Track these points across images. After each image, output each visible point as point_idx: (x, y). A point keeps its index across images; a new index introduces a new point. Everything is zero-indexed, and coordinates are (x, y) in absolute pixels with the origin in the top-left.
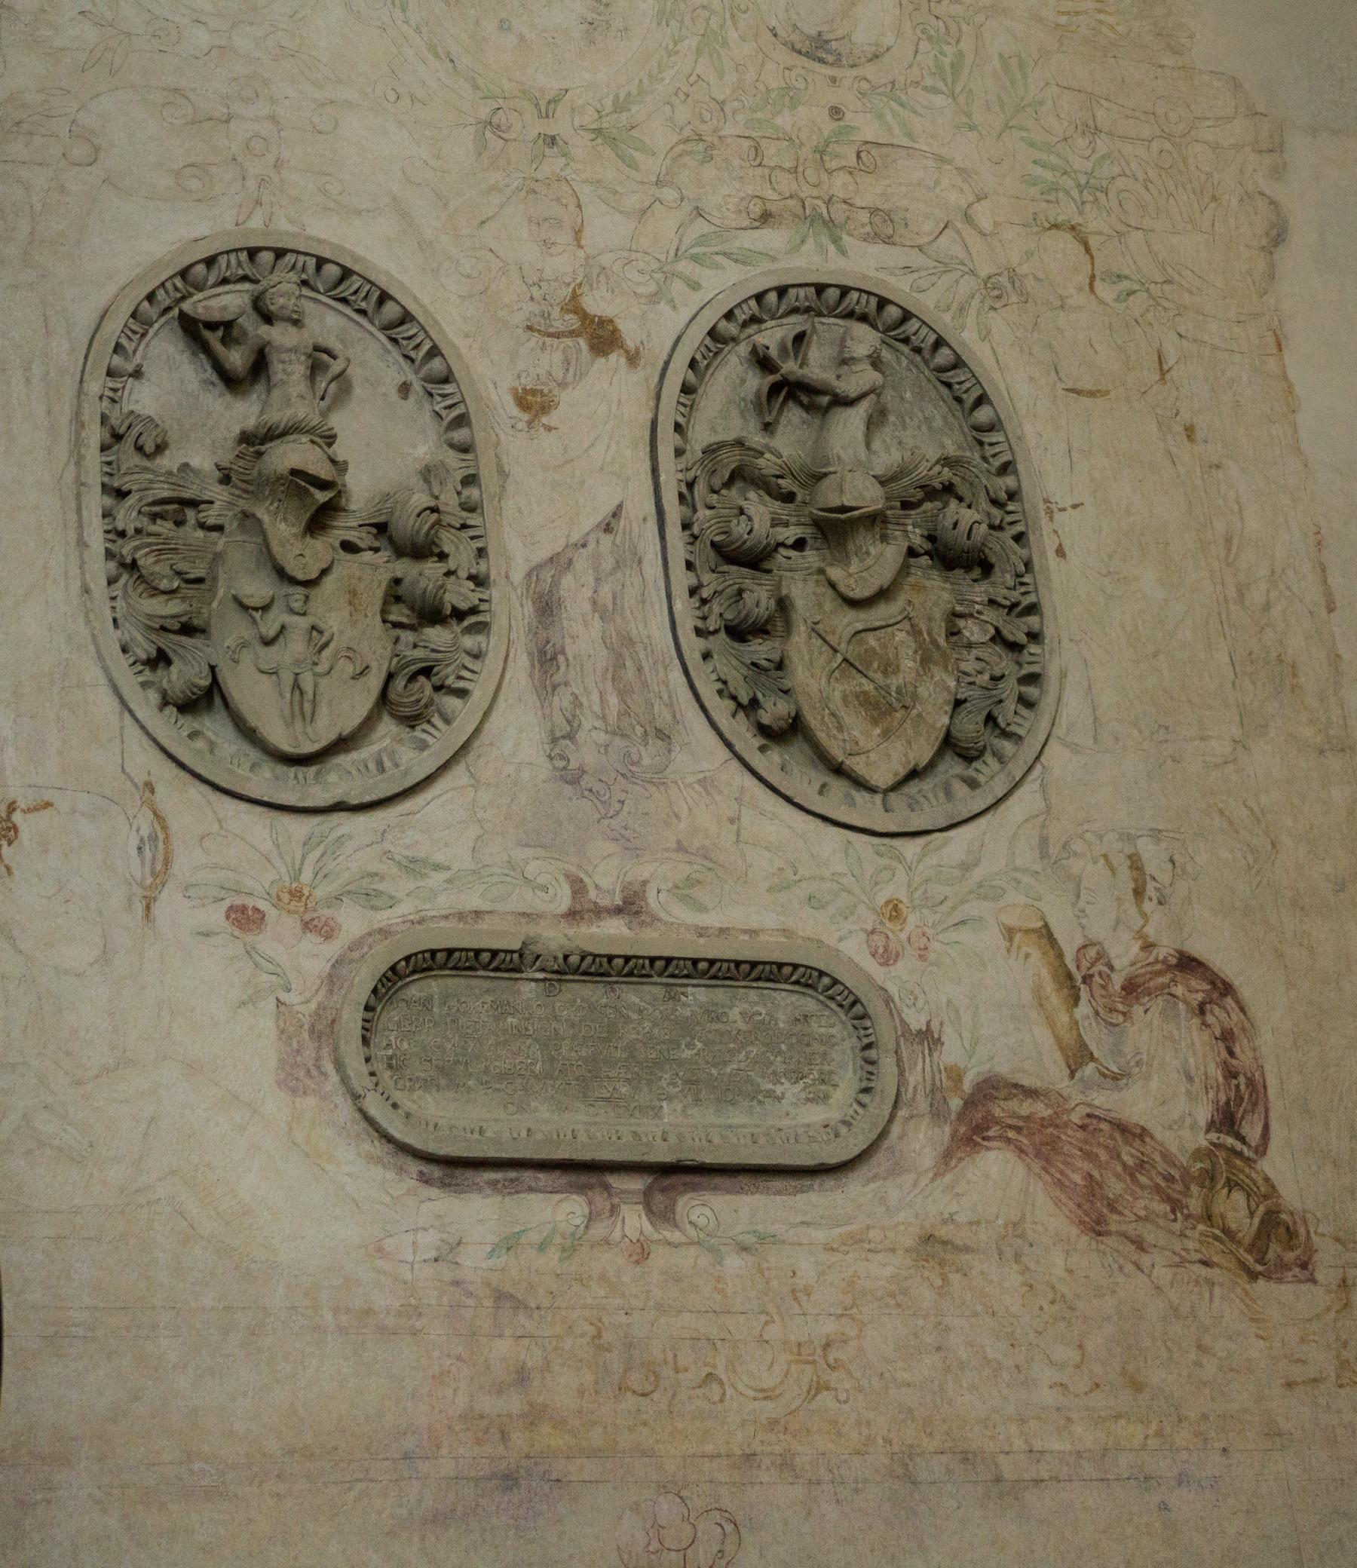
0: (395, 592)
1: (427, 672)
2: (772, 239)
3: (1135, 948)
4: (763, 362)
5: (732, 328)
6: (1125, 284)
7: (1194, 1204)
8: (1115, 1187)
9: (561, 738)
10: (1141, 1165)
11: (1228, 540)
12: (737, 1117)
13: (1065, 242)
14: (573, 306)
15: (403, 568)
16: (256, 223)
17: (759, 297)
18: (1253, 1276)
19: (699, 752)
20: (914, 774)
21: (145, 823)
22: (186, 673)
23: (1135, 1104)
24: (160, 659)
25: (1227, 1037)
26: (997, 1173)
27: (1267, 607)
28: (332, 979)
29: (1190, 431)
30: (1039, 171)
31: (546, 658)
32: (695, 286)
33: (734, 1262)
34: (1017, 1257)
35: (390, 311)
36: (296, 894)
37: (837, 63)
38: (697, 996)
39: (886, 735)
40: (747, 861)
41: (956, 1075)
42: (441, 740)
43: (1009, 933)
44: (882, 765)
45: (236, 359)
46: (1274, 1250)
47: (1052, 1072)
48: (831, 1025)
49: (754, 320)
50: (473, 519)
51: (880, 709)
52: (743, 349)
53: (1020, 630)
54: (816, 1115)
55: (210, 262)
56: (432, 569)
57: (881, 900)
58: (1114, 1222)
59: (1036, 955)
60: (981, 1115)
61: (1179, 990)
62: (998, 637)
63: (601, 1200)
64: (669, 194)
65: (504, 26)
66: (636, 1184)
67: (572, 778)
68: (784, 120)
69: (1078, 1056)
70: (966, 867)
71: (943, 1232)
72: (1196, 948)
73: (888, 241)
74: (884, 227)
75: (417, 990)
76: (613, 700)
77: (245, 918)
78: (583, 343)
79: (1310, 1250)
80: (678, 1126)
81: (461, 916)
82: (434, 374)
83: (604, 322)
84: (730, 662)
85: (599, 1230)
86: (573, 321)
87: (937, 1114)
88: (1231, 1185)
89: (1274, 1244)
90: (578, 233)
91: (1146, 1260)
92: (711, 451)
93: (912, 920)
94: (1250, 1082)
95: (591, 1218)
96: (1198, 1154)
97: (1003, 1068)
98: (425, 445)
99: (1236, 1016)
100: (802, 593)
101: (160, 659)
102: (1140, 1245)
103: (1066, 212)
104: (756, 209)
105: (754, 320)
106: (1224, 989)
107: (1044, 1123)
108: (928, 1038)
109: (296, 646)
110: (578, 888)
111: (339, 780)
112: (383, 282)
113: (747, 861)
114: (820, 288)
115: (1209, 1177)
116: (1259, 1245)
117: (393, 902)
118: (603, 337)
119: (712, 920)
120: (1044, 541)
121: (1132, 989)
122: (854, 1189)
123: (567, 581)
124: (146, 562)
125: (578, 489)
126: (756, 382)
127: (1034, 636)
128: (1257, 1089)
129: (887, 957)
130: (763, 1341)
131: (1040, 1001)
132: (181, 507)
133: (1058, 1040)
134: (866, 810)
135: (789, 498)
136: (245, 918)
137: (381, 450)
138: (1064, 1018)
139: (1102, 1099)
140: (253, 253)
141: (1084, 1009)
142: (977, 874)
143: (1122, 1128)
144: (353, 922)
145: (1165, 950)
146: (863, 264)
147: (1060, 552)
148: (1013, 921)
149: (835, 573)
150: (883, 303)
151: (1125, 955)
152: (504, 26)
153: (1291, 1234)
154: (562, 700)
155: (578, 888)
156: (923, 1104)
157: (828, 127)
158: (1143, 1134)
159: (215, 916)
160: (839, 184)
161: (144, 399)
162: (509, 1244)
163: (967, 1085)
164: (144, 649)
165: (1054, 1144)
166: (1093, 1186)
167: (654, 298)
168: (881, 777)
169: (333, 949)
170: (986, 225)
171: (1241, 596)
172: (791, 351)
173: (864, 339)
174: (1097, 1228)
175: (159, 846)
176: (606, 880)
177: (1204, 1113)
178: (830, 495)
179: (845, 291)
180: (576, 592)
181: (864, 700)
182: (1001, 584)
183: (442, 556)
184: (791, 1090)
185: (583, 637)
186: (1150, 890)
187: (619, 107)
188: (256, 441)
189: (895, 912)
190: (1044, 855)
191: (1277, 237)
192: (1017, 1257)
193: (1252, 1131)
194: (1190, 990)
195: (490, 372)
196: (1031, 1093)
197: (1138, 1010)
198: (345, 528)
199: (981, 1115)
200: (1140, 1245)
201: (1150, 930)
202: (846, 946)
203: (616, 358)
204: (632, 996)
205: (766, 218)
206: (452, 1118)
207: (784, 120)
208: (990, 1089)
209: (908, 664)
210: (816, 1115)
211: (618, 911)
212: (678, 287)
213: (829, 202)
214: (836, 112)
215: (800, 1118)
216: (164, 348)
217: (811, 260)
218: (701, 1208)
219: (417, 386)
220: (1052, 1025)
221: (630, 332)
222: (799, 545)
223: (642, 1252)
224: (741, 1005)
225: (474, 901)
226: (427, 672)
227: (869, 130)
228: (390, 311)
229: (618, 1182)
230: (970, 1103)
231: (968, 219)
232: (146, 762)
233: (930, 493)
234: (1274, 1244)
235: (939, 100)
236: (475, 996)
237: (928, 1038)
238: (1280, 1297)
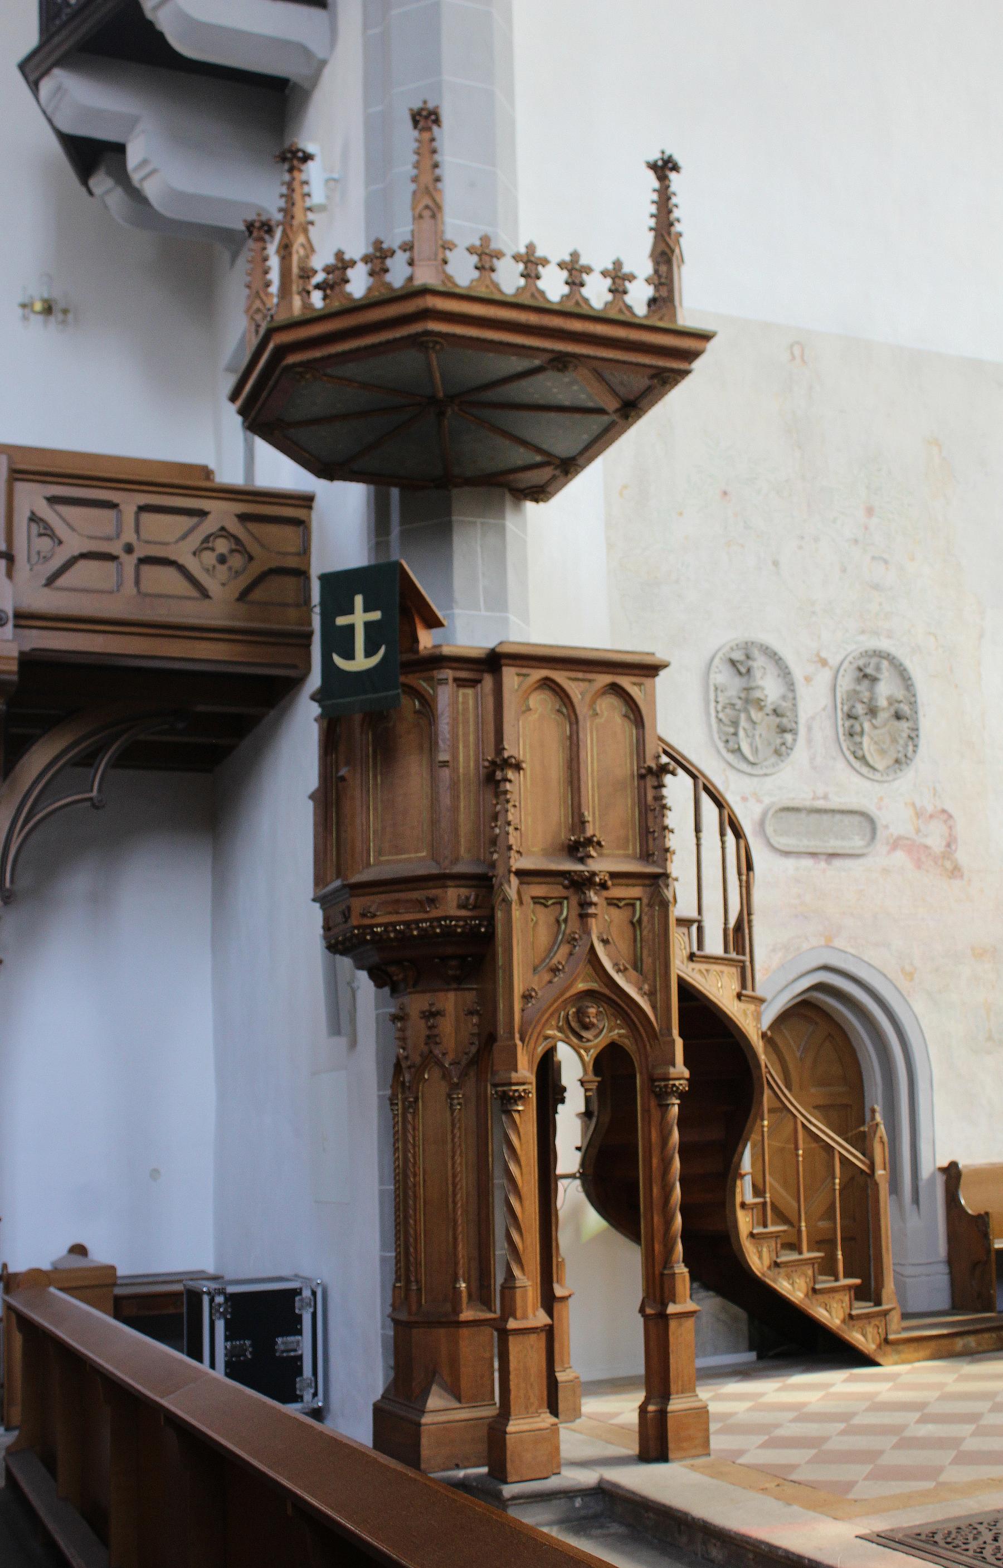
2: (862, 638)
9: (812, 759)
14: (818, 655)
19: (841, 764)
22: (732, 745)
23: (929, 841)
25: (950, 828)
26: (900, 857)
31: (809, 741)
38: (838, 817)
40: (850, 788)
43: (906, 804)
44: (880, 765)
45: (743, 670)
60: (896, 844)
69: (918, 831)
72: (946, 808)
80: (834, 844)
82: (785, 673)
89: (955, 872)
100: (867, 726)
108: (886, 827)
110: (814, 792)
113: (850, 788)
116: (952, 872)
118: (824, 663)
120: (921, 713)
121: (931, 816)
127: (917, 736)
143: (926, 847)
146: (884, 644)
151: (930, 809)
155: (814, 792)
166: (919, 859)
176: (820, 792)
177: (944, 843)
184: (857, 838)
189: (881, 799)
193: (953, 847)
194: (944, 817)
195: (798, 673)
196: (907, 839)
199: (896, 844)
200: (927, 871)
202: (871, 809)
203: (827, 669)
204: (825, 817)
208: (900, 838)
215: (857, 843)
237: (886, 827)
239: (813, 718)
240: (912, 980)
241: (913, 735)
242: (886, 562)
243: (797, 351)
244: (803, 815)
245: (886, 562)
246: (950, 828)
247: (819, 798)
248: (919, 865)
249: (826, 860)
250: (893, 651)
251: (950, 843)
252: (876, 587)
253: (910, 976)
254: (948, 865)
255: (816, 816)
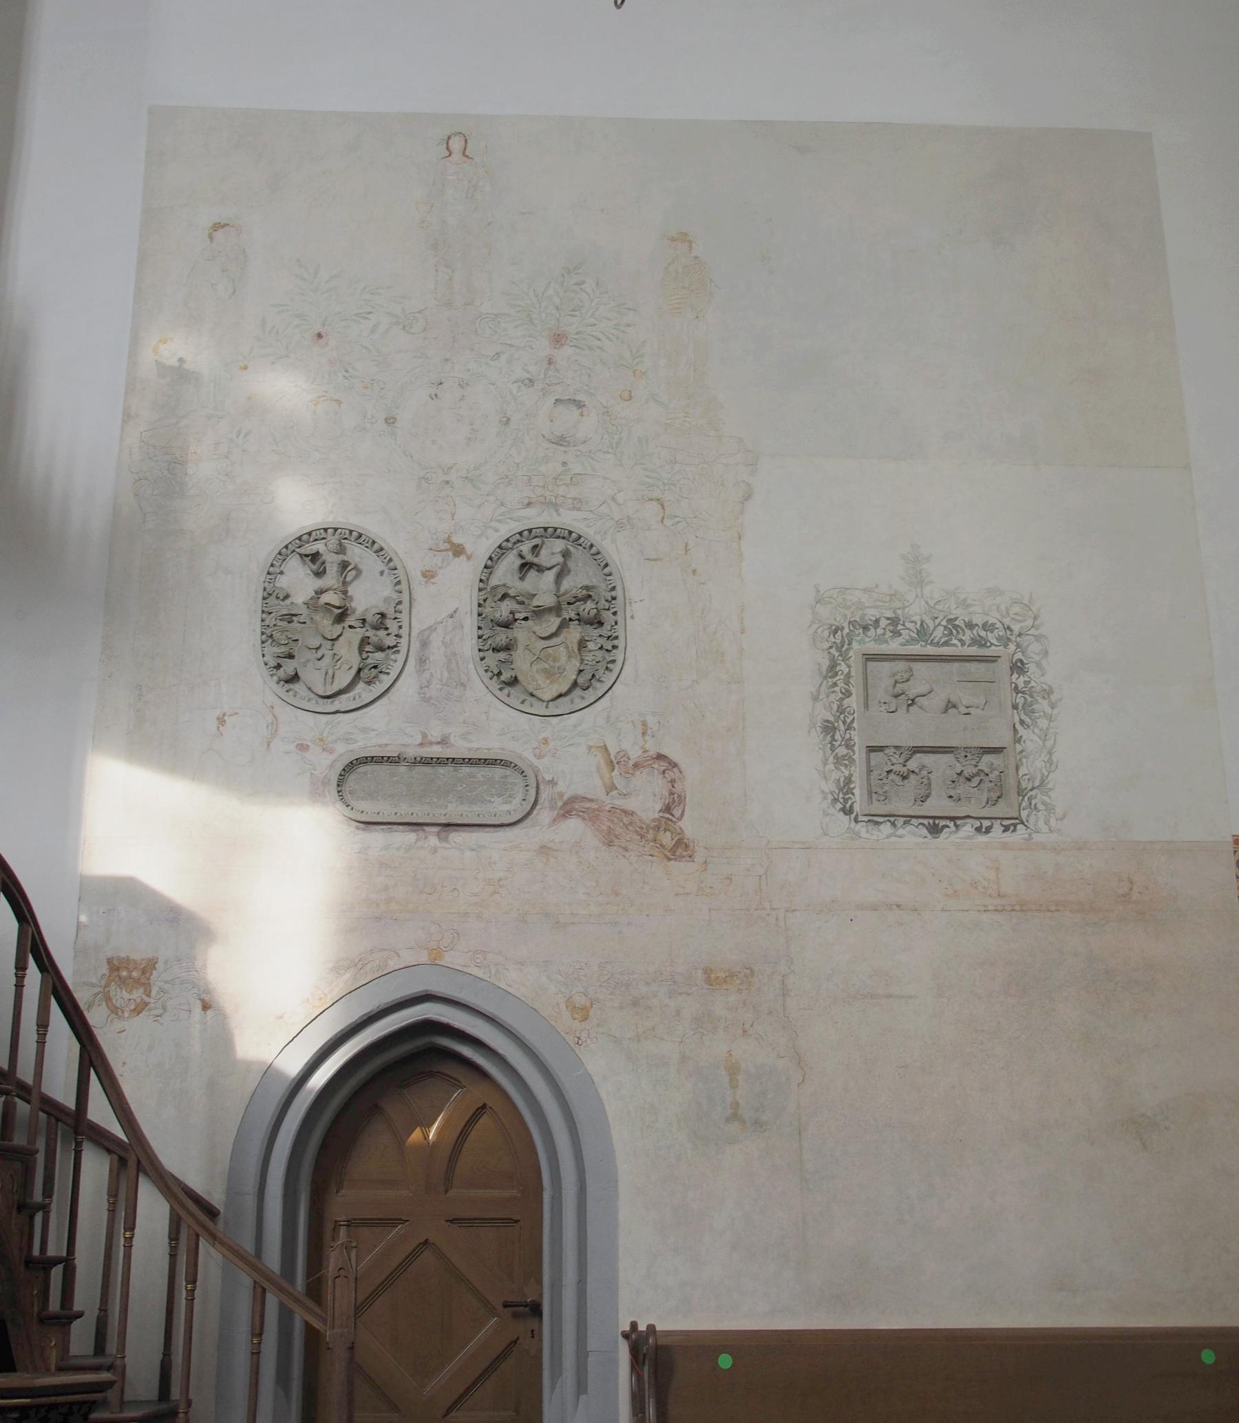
0: (364, 641)
1: (375, 667)
2: (531, 512)
3: (640, 752)
4: (521, 556)
5: (510, 545)
6: (677, 519)
7: (650, 836)
8: (619, 830)
10: (631, 823)
11: (703, 610)
12: (476, 808)
13: (655, 506)
14: (448, 541)
15: (370, 633)
16: (330, 519)
17: (521, 533)
18: (670, 860)
20: (560, 696)
21: (270, 718)
23: (630, 804)
24: (279, 666)
25: (673, 781)
26: (574, 826)
27: (715, 632)
28: (331, 766)
29: (694, 572)
30: (647, 480)
31: (422, 661)
32: (497, 531)
33: (468, 854)
34: (577, 853)
35: (376, 547)
36: (321, 740)
37: (568, 445)
38: (465, 770)
39: (551, 683)
40: (493, 724)
41: (561, 795)
42: (378, 688)
43: (590, 748)
46: (679, 851)
47: (600, 794)
48: (515, 778)
49: (519, 541)
50: (398, 615)
51: (549, 674)
52: (515, 552)
53: (611, 644)
54: (506, 807)
55: (310, 534)
56: (382, 633)
57: (541, 737)
58: (617, 842)
59: (599, 755)
60: (568, 808)
61: (656, 766)
62: (601, 648)
63: (421, 834)
64: (492, 498)
65: (434, 442)
66: (435, 829)
67: (426, 700)
68: (543, 469)
69: (611, 788)
70: (575, 726)
71: (550, 845)
72: (665, 752)
73: (579, 509)
74: (578, 504)
75: (362, 769)
76: (446, 675)
77: (302, 748)
78: (450, 553)
79: (694, 851)
80: (454, 811)
81: (380, 746)
82: (391, 565)
83: (459, 545)
84: (492, 659)
85: (420, 844)
86: (447, 546)
87: (552, 808)
88: (665, 830)
89: (680, 848)
90: (453, 515)
91: (627, 854)
92: (496, 587)
93: (552, 744)
94: (679, 796)
95: (417, 840)
96: (654, 820)
97: (581, 792)
98: (388, 591)
99: (678, 774)
101: (279, 666)
102: (626, 849)
103: (656, 494)
104: (526, 501)
105: (519, 541)
106: (675, 765)
107: (594, 810)
109: (327, 660)
110: (424, 735)
111: (343, 702)
112: (373, 537)
113: (493, 724)
114: (546, 529)
115: (657, 828)
116: (673, 850)
117: (356, 741)
118: (458, 551)
119: (474, 745)
121: (636, 766)
122: (516, 830)
123: (434, 635)
124: (276, 635)
125: (445, 607)
126: (519, 562)
128: (681, 799)
129: (539, 757)
130: (476, 878)
131: (598, 769)
132: (290, 617)
133: (604, 784)
134: (539, 708)
135: (522, 603)
136: (302, 748)
137: (368, 595)
138: (608, 776)
139: (619, 802)
140: (326, 530)
141: (616, 772)
142: (580, 728)
143: (625, 812)
144: (341, 748)
145: (652, 753)
146: (567, 519)
147: (632, 617)
148: (591, 744)
149: (536, 628)
150: (570, 532)
151: (635, 754)
152: (434, 442)
153: (687, 846)
154: (427, 675)
155: (424, 735)
156: (547, 804)
157: (560, 469)
158: (633, 813)
159: (292, 747)
160: (561, 491)
161: (283, 582)
162: (387, 848)
163: (565, 798)
164: (273, 663)
165: (597, 817)
167: (479, 536)
168: (547, 697)
169: (332, 757)
170: (621, 501)
171: (705, 629)
172: (527, 550)
173: (559, 545)
174: (610, 844)
175: (274, 724)
176: (435, 733)
177: (658, 806)
178: (536, 602)
179: (556, 529)
180: (436, 639)
181: (545, 671)
182: (605, 631)
183: (387, 629)
184: (497, 800)
185: (437, 653)
186: (649, 732)
187: (476, 468)
188: (320, 592)
189: (546, 741)
190: (608, 721)
191: (747, 497)
192: (577, 853)
193: (677, 812)
194: (664, 765)
196: (591, 800)
197: (638, 773)
198: (351, 620)
199: (568, 808)
201: (647, 746)
202: (524, 752)
203: (463, 558)
204: (441, 770)
205: (529, 504)
206: (371, 809)
207: (543, 469)
208: (574, 799)
209: (564, 658)
210: (506, 807)
211: (439, 743)
212: (490, 531)
213: (556, 497)
214: (564, 464)
216: (294, 563)
217: (538, 518)
218: (458, 837)
219: (386, 571)
220: (602, 778)
221: (469, 549)
222: (526, 619)
223: (435, 851)
224: (481, 773)
225: (385, 741)
226: (375, 667)
227: (577, 469)
228: (376, 547)
229: (426, 828)
230: (565, 804)
231: (613, 499)
232: (271, 699)
233: (577, 599)
234: (680, 848)
235: (609, 456)
236: (384, 769)
237: (552, 783)
238: (678, 868)
239: (432, 629)
240: (585, 1018)
241: (608, 646)
242: (580, 405)
243: (456, 144)
244: (402, 769)
245: (580, 405)
246: (673, 781)
247: (431, 743)
248: (609, 840)
249: (438, 834)
250: (579, 527)
251: (672, 806)
252: (561, 441)
253: (583, 1013)
254: (667, 839)
255: (427, 770)
